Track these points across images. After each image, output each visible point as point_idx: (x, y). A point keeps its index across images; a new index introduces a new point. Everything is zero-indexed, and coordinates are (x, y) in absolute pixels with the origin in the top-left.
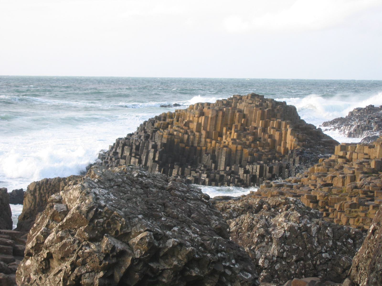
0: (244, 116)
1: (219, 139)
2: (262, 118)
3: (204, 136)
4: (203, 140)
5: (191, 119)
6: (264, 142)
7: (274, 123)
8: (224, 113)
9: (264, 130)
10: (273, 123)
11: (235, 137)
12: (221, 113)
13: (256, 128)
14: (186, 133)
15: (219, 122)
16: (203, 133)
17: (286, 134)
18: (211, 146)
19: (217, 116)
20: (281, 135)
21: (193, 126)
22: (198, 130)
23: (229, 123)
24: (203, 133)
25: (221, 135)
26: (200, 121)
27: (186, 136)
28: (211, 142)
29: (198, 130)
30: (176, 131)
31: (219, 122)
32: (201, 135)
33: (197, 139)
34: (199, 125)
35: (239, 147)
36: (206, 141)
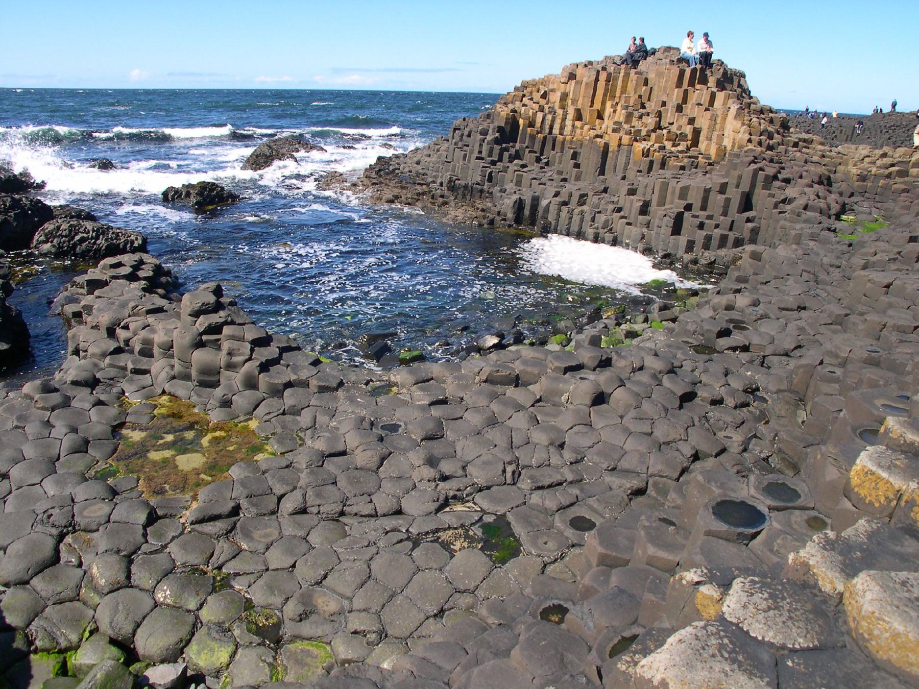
0: (646, 83)
2: (679, 84)
3: (570, 116)
4: (569, 123)
6: (678, 132)
7: (700, 94)
8: (609, 75)
9: (679, 109)
11: (622, 119)
12: (603, 76)
14: (541, 109)
17: (724, 118)
19: (597, 80)
20: (714, 119)
25: (600, 116)
27: (540, 116)
28: (582, 128)
30: (524, 105)
34: (564, 97)
35: (626, 139)
36: (573, 126)
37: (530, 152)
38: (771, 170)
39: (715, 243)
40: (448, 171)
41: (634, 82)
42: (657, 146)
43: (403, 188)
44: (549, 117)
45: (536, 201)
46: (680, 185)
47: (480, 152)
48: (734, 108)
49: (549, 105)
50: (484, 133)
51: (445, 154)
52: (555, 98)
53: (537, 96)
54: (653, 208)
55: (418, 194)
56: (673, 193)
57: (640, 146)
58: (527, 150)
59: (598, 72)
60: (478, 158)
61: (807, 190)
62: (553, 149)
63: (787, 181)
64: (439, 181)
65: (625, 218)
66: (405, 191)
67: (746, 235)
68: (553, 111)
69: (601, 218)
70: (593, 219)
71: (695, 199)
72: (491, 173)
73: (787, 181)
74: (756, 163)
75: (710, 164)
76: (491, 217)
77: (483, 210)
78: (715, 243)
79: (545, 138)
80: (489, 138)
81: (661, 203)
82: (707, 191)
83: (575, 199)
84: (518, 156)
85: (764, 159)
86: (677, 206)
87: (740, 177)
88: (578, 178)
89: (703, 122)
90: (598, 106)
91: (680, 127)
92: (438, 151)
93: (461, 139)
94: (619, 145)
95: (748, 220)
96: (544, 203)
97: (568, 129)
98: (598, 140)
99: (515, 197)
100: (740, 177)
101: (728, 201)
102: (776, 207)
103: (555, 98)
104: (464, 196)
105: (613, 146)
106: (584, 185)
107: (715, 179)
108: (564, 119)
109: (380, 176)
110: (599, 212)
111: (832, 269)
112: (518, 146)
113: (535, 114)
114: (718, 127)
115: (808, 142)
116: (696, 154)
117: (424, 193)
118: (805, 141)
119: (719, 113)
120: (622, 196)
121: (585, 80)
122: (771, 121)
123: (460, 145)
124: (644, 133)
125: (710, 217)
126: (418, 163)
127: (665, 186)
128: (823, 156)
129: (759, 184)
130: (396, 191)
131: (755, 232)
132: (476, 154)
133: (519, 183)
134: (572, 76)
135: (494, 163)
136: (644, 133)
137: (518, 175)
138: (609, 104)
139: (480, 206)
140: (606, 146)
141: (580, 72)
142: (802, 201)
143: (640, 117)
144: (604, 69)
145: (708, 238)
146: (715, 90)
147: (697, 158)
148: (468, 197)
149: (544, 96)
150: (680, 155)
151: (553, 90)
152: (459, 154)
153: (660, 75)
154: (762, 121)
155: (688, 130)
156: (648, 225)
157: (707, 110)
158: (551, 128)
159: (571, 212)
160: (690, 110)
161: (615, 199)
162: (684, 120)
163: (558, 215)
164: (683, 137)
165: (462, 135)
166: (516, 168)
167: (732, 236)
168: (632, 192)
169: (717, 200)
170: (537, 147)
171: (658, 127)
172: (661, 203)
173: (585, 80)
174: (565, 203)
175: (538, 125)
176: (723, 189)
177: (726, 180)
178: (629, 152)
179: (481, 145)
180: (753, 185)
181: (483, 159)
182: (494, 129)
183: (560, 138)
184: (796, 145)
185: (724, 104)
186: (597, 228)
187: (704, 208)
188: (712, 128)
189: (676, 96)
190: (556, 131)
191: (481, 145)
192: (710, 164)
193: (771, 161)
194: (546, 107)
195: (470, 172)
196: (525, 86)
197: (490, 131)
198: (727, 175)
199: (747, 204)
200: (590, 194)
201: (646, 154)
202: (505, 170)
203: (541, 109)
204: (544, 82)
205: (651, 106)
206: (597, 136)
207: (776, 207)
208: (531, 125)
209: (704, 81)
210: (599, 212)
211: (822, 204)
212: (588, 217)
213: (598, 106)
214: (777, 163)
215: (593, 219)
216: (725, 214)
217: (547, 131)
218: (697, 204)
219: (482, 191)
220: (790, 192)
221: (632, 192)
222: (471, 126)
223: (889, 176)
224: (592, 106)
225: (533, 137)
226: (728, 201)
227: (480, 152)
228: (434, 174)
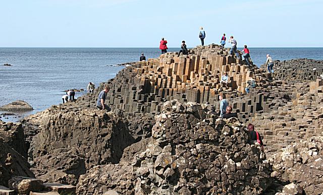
0: (208, 63)
1: (187, 81)
2: (224, 63)
3: (174, 79)
4: (174, 82)
5: (163, 66)
7: (233, 67)
8: (191, 60)
10: (233, 68)
11: (202, 80)
12: (188, 61)
14: (160, 76)
15: (187, 68)
16: (174, 77)
17: (245, 77)
18: (181, 87)
19: (185, 62)
20: (241, 77)
21: (166, 71)
22: (170, 74)
23: (195, 68)
24: (174, 77)
25: (188, 79)
26: (171, 68)
27: (160, 80)
28: (181, 84)
29: (170, 74)
30: (151, 75)
31: (187, 68)
32: (172, 78)
34: (170, 70)
35: (207, 88)
36: (176, 83)
37: (157, 97)
38: (266, 95)
41: (202, 62)
42: (219, 90)
46: (233, 103)
47: (134, 98)
48: (249, 72)
57: (213, 90)
58: (156, 96)
59: (185, 59)
61: (279, 100)
62: (168, 95)
71: (240, 108)
73: (273, 98)
75: (243, 95)
79: (164, 90)
80: (139, 91)
82: (244, 104)
84: (152, 99)
85: (263, 91)
87: (255, 98)
89: (237, 79)
94: (204, 90)
100: (255, 98)
101: (252, 107)
102: (269, 107)
103: (166, 71)
105: (202, 91)
107: (247, 99)
108: (171, 80)
112: (151, 94)
113: (157, 79)
114: (243, 80)
115: (281, 83)
116: (235, 92)
118: (278, 83)
119: (243, 75)
121: (179, 63)
122: (264, 76)
124: (213, 85)
125: (246, 114)
128: (286, 89)
135: (143, 102)
136: (213, 85)
138: (192, 73)
140: (199, 91)
142: (278, 103)
143: (210, 79)
146: (239, 65)
147: (236, 93)
150: (230, 93)
153: (214, 59)
154: (260, 77)
157: (237, 73)
158: (166, 85)
169: (248, 107)
171: (218, 82)
173: (179, 63)
176: (250, 103)
178: (209, 93)
179: (135, 95)
180: (260, 101)
183: (171, 89)
184: (275, 85)
185: (244, 70)
187: (244, 110)
188: (240, 81)
190: (168, 86)
191: (135, 95)
192: (243, 95)
193: (266, 91)
194: (162, 75)
198: (250, 98)
201: (216, 93)
202: (150, 105)
205: (213, 73)
207: (269, 107)
208: (156, 84)
209: (234, 61)
213: (186, 74)
214: (268, 92)
217: (164, 86)
218: (241, 109)
220: (274, 101)
224: (184, 74)
225: (157, 90)
226: (252, 107)
227: (134, 98)
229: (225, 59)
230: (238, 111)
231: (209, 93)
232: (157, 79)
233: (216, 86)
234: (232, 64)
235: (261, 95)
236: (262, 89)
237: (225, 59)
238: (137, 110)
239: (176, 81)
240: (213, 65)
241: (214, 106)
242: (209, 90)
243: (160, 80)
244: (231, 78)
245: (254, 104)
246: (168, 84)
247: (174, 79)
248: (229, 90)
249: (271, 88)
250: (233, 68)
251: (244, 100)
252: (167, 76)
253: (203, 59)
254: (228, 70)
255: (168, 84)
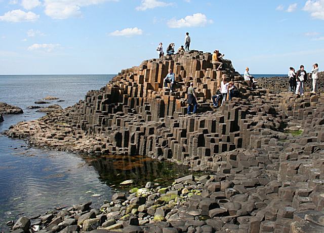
0: (182, 68)
2: (198, 68)
3: (145, 88)
4: (145, 91)
6: (199, 92)
7: (208, 73)
8: (163, 65)
9: (199, 81)
12: (161, 66)
13: (191, 79)
14: (130, 84)
16: (145, 84)
20: (215, 84)
22: (141, 82)
24: (145, 84)
27: (129, 88)
28: (151, 93)
29: (141, 82)
30: (121, 83)
32: (142, 87)
33: (139, 90)
34: (142, 77)
35: (172, 98)
36: (147, 91)
37: (125, 107)
38: (244, 109)
39: (220, 149)
40: (82, 119)
41: (176, 69)
43: (57, 129)
44: (134, 88)
45: (127, 133)
46: (200, 120)
47: (98, 109)
49: (135, 82)
50: (101, 98)
51: (81, 110)
52: (137, 78)
53: (128, 78)
54: (188, 132)
55: (66, 133)
56: (197, 124)
57: (178, 101)
59: (158, 65)
60: (97, 112)
62: (138, 104)
63: (254, 113)
64: (77, 125)
65: (175, 139)
66: (59, 131)
67: (236, 143)
68: (136, 85)
69: (161, 141)
70: (157, 141)
71: (208, 127)
72: (104, 119)
73: (254, 113)
74: (237, 106)
76: (104, 143)
77: (99, 140)
78: (220, 149)
79: (133, 99)
80: (103, 100)
81: (192, 130)
82: (214, 123)
83: (147, 132)
84: (120, 109)
85: (241, 103)
86: (198, 132)
87: (229, 114)
88: (149, 119)
90: (159, 81)
91: (199, 90)
92: (79, 108)
93: (90, 102)
94: (169, 101)
95: (236, 135)
96: (131, 134)
97: (145, 94)
98: (158, 99)
99: (116, 132)
100: (229, 114)
101: (224, 126)
102: (248, 128)
104: (91, 133)
105: (166, 102)
106: (152, 123)
107: (219, 114)
109: (47, 123)
110: (161, 137)
111: (273, 160)
113: (127, 87)
115: (265, 92)
117: (69, 132)
119: (218, 82)
120: (172, 128)
121: (151, 69)
123: (89, 105)
124: (181, 94)
125: (217, 136)
126: (68, 115)
127: (192, 121)
128: (271, 99)
129: (240, 117)
130: (54, 132)
131: (240, 141)
132: (96, 110)
133: (119, 124)
134: (145, 67)
136: (181, 94)
137: (118, 120)
139: (98, 138)
140: (163, 102)
141: (149, 64)
142: (261, 123)
144: (160, 62)
145: (216, 147)
148: (93, 133)
149: (132, 77)
151: (136, 75)
152: (88, 110)
153: (188, 64)
154: (240, 84)
155: (204, 91)
156: (186, 142)
157: (212, 80)
159: (146, 138)
160: (205, 81)
161: (169, 130)
162: (201, 86)
163: (139, 141)
164: (202, 95)
165: (91, 99)
166: (117, 116)
167: (229, 144)
168: (177, 125)
170: (129, 104)
172: (192, 130)
173: (151, 69)
174: (143, 134)
175: (129, 93)
177: (223, 116)
178: (174, 104)
179: (99, 106)
181: (100, 112)
182: (105, 96)
186: (160, 146)
187: (213, 131)
189: (196, 74)
190: (139, 95)
191: (99, 106)
193: (245, 104)
195: (94, 120)
196: (123, 72)
197: (104, 97)
199: (235, 126)
200: (155, 128)
202: (112, 117)
203: (130, 84)
204: (132, 70)
206: (157, 97)
208: (126, 92)
209: (211, 66)
210: (161, 137)
211: (271, 124)
212: (155, 141)
213: (159, 81)
214: (248, 104)
215: (157, 141)
216: (224, 133)
217: (134, 95)
218: (210, 129)
219: (99, 130)
221: (177, 125)
222: (95, 94)
223: (302, 106)
224: (156, 81)
225: (126, 99)
227: (98, 109)
228: (75, 121)
229: (198, 63)
230: (206, 132)
231: (174, 104)
232: (127, 87)
233: (184, 95)
234: (207, 69)
235: (237, 110)
236: (239, 100)
237: (198, 63)
238: (98, 123)
239: (147, 89)
240: (187, 71)
241: (178, 122)
242: (174, 101)
243: (129, 88)
244: (204, 85)
245: (227, 123)
246: (139, 93)
247: (145, 88)
248: (200, 101)
249: (253, 98)
250: (208, 74)
251: (215, 115)
252: (138, 83)
253: (177, 64)
254: (202, 75)
255: (139, 93)
